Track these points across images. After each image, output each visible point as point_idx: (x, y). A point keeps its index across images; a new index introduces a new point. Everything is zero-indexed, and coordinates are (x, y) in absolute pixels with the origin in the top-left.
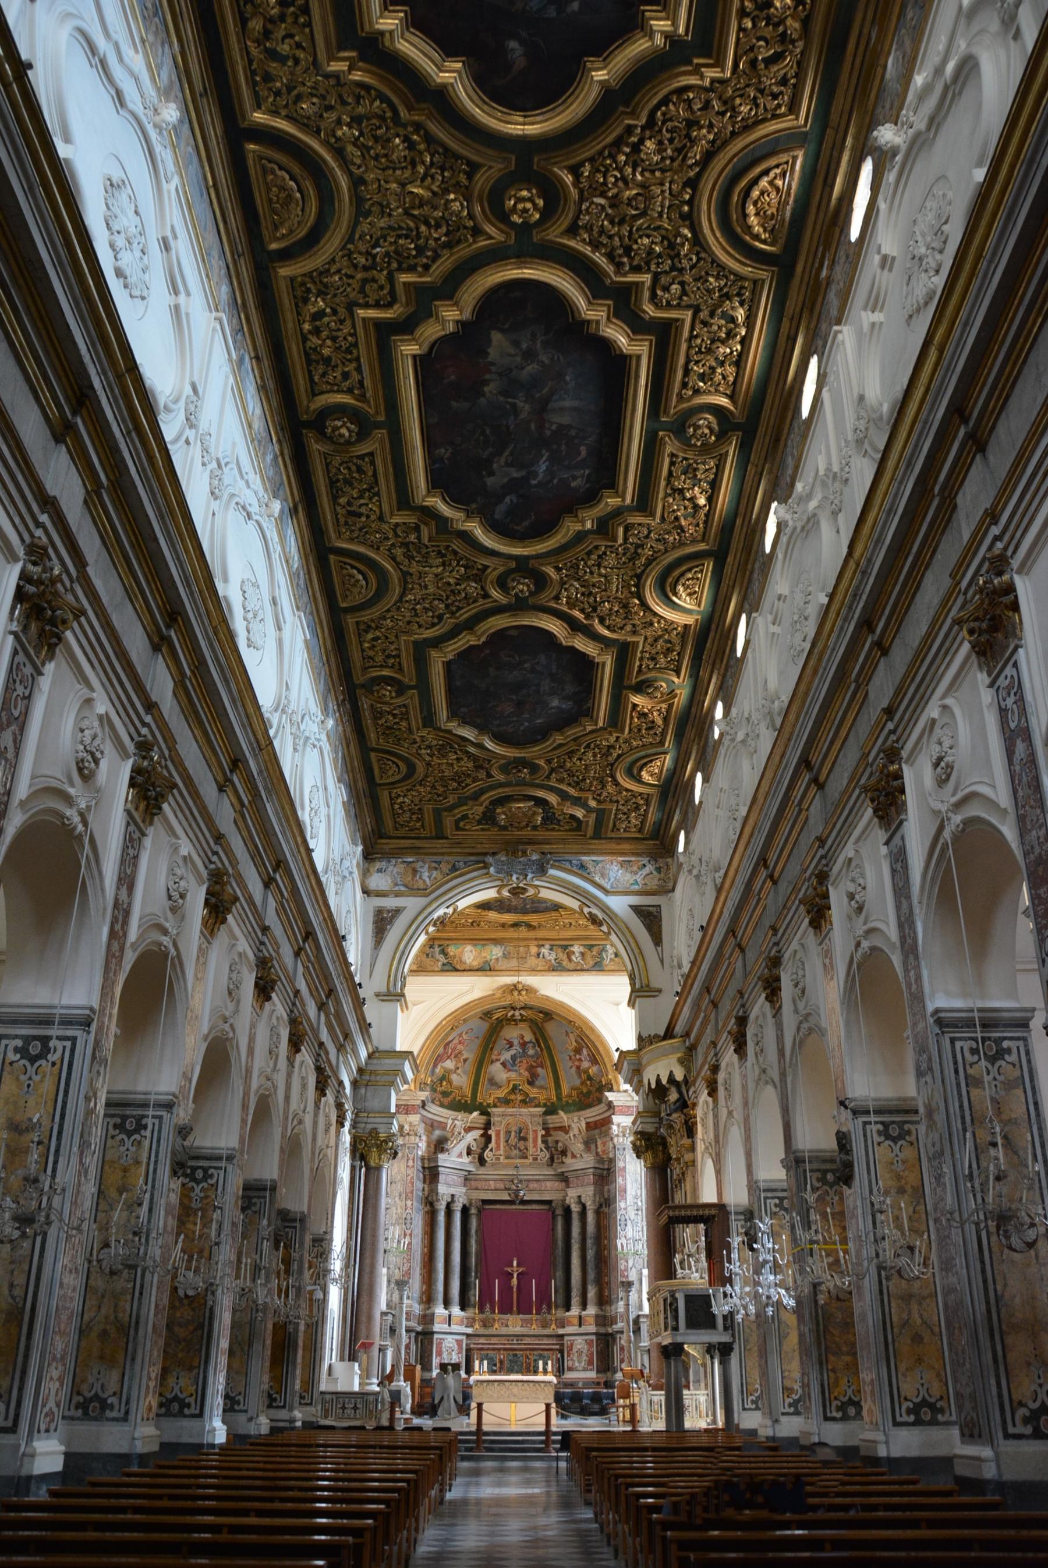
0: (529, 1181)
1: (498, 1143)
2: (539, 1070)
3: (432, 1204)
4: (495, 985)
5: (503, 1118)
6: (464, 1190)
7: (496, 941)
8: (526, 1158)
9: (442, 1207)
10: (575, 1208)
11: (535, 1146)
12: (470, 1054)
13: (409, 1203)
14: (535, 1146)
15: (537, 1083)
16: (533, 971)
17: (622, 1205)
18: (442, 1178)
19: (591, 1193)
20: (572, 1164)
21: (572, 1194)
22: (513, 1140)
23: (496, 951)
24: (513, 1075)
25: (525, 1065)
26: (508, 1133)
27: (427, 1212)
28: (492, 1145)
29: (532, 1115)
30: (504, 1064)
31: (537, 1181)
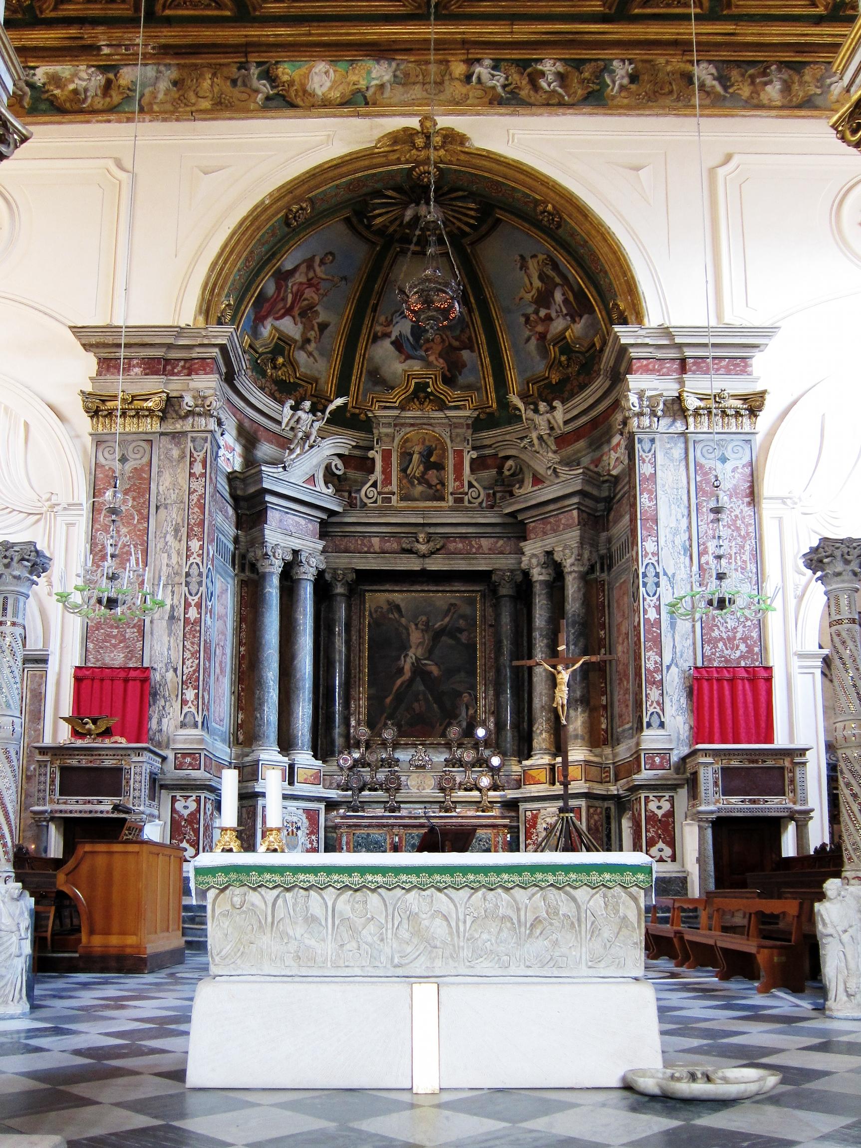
0: (446, 536)
1: (386, 472)
2: (466, 354)
3: (253, 567)
4: (378, 133)
5: (398, 426)
6: (320, 545)
7: (380, 51)
8: (442, 498)
9: (275, 568)
10: (539, 575)
11: (459, 476)
12: (334, 316)
13: (195, 544)
14: (459, 476)
15: (461, 380)
16: (458, 105)
17: (650, 546)
18: (273, 516)
19: (574, 544)
20: (530, 493)
21: (533, 548)
22: (416, 467)
23: (379, 72)
24: (416, 366)
25: (438, 348)
26: (406, 456)
27: (243, 584)
28: (378, 475)
29: (453, 426)
30: (397, 344)
31: (463, 537)
